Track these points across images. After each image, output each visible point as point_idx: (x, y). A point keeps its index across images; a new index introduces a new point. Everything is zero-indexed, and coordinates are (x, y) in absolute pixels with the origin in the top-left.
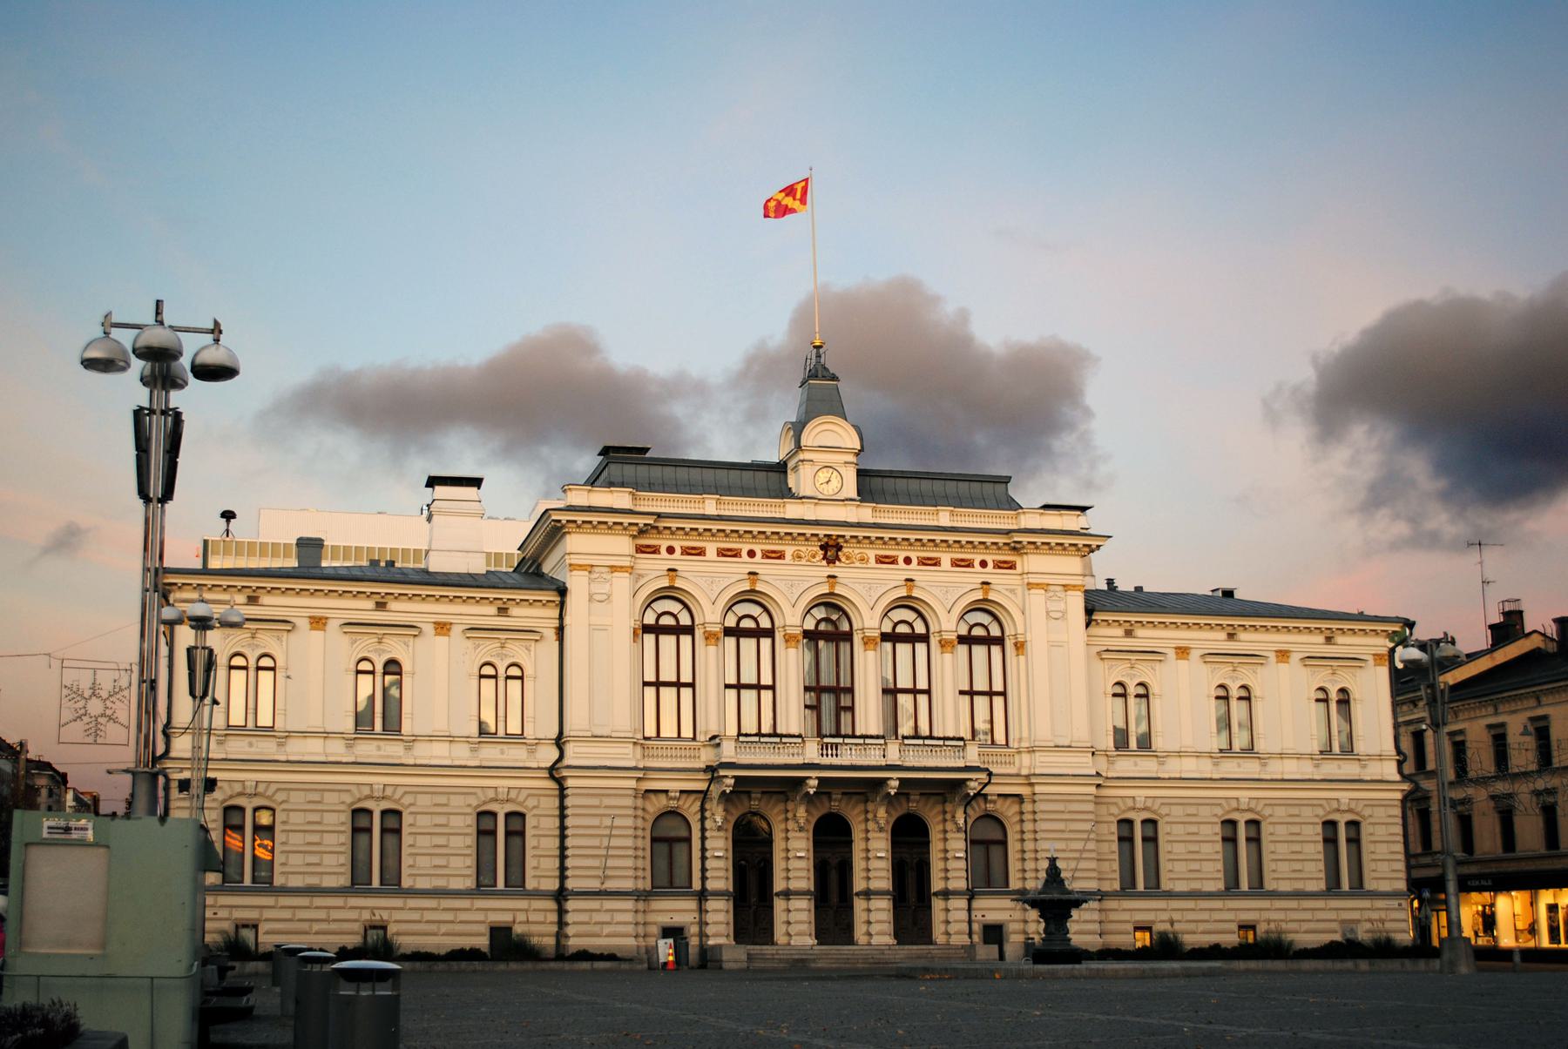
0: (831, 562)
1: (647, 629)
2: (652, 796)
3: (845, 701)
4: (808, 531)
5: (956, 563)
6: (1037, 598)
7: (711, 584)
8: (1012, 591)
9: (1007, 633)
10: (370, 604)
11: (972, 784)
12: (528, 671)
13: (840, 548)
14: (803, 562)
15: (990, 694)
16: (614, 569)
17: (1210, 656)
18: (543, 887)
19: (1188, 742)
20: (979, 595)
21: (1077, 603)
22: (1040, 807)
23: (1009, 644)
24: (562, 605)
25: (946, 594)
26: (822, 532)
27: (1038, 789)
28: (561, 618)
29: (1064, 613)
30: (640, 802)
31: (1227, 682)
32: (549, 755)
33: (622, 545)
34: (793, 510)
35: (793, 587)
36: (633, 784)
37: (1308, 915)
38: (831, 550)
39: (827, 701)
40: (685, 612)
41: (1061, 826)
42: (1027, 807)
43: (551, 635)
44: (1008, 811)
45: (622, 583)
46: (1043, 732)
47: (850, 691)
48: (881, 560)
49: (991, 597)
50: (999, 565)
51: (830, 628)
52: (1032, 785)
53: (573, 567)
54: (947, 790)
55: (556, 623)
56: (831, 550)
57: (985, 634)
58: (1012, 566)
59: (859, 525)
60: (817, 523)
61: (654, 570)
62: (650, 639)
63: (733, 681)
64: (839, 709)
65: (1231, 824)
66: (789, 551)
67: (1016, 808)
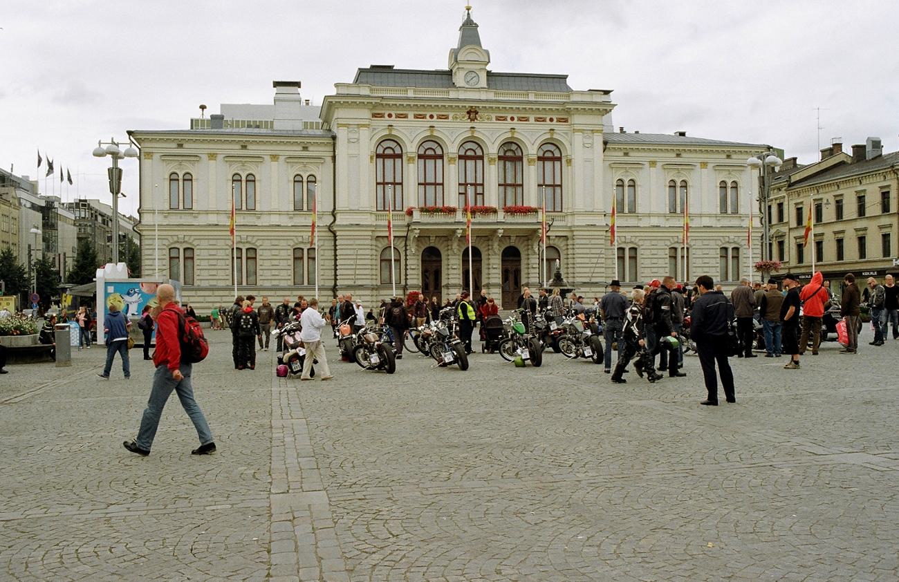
0: (472, 120)
1: (378, 156)
2: (381, 239)
3: (479, 190)
4: (461, 105)
5: (537, 120)
6: (578, 138)
7: (411, 134)
10: (238, 147)
11: (458, 231)
12: (318, 178)
13: (477, 113)
14: (458, 120)
16: (359, 126)
17: (668, 166)
18: (327, 284)
19: (655, 210)
20: (548, 136)
21: (598, 140)
22: (577, 241)
24: (334, 145)
25: (531, 138)
26: (467, 105)
27: (575, 233)
28: (334, 151)
29: (592, 144)
30: (374, 242)
31: (676, 179)
32: (330, 220)
33: (365, 114)
34: (453, 94)
35: (452, 134)
36: (370, 233)
37: (218, 299)
38: (472, 113)
39: (470, 190)
40: (398, 147)
41: (587, 251)
42: (570, 242)
43: (329, 160)
44: (560, 244)
45: (364, 133)
46: (580, 205)
47: (482, 185)
48: (498, 119)
50: (559, 120)
51: (433, 153)
52: (572, 231)
53: (339, 125)
54: (530, 235)
55: (332, 154)
56: (472, 113)
57: (552, 155)
58: (566, 121)
59: (487, 101)
60: (465, 100)
61: (382, 124)
62: (380, 161)
63: (423, 181)
64: (476, 194)
66: (451, 115)
67: (564, 243)
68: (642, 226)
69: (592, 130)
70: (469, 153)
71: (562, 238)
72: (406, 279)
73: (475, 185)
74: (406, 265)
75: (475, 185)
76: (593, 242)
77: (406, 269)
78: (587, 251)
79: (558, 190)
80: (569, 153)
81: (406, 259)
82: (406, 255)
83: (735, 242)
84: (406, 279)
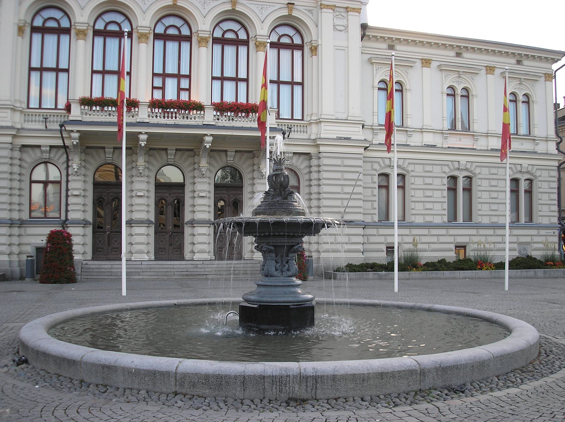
8: (310, 11)
9: (305, 41)
15: (292, 83)
19: (429, 123)
20: (285, 12)
23: (306, 49)
29: (346, 27)
47: (189, 77)
49: (295, 13)
65: (454, 178)
67: (306, 163)
68: (413, 144)
69: (347, 8)
70: (171, 31)
71: (302, 157)
72: (67, 211)
73: (178, 76)
74: (67, 190)
75: (178, 76)
76: (347, 162)
77: (67, 196)
78: (338, 175)
79: (298, 89)
80: (314, 38)
81: (68, 181)
82: (68, 175)
83: (528, 172)
84: (67, 211)
